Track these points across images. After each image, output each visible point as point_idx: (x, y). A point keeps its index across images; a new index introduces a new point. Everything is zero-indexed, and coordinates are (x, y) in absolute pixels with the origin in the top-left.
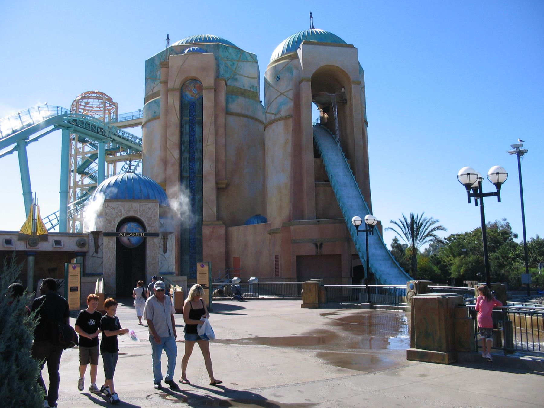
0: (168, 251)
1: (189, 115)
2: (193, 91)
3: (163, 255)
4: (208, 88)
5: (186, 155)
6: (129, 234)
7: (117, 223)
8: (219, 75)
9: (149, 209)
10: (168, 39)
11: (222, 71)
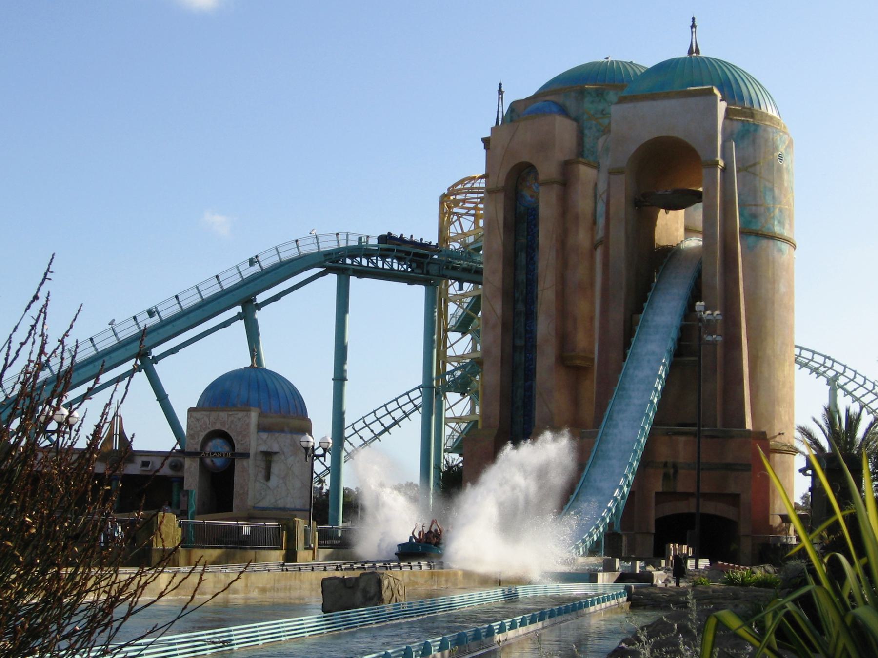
0: (272, 477)
1: (526, 233)
2: (534, 187)
3: (264, 484)
4: (546, 183)
5: (521, 307)
6: (212, 453)
7: (201, 438)
8: (583, 151)
9: (239, 419)
10: (501, 92)
11: (588, 142)
